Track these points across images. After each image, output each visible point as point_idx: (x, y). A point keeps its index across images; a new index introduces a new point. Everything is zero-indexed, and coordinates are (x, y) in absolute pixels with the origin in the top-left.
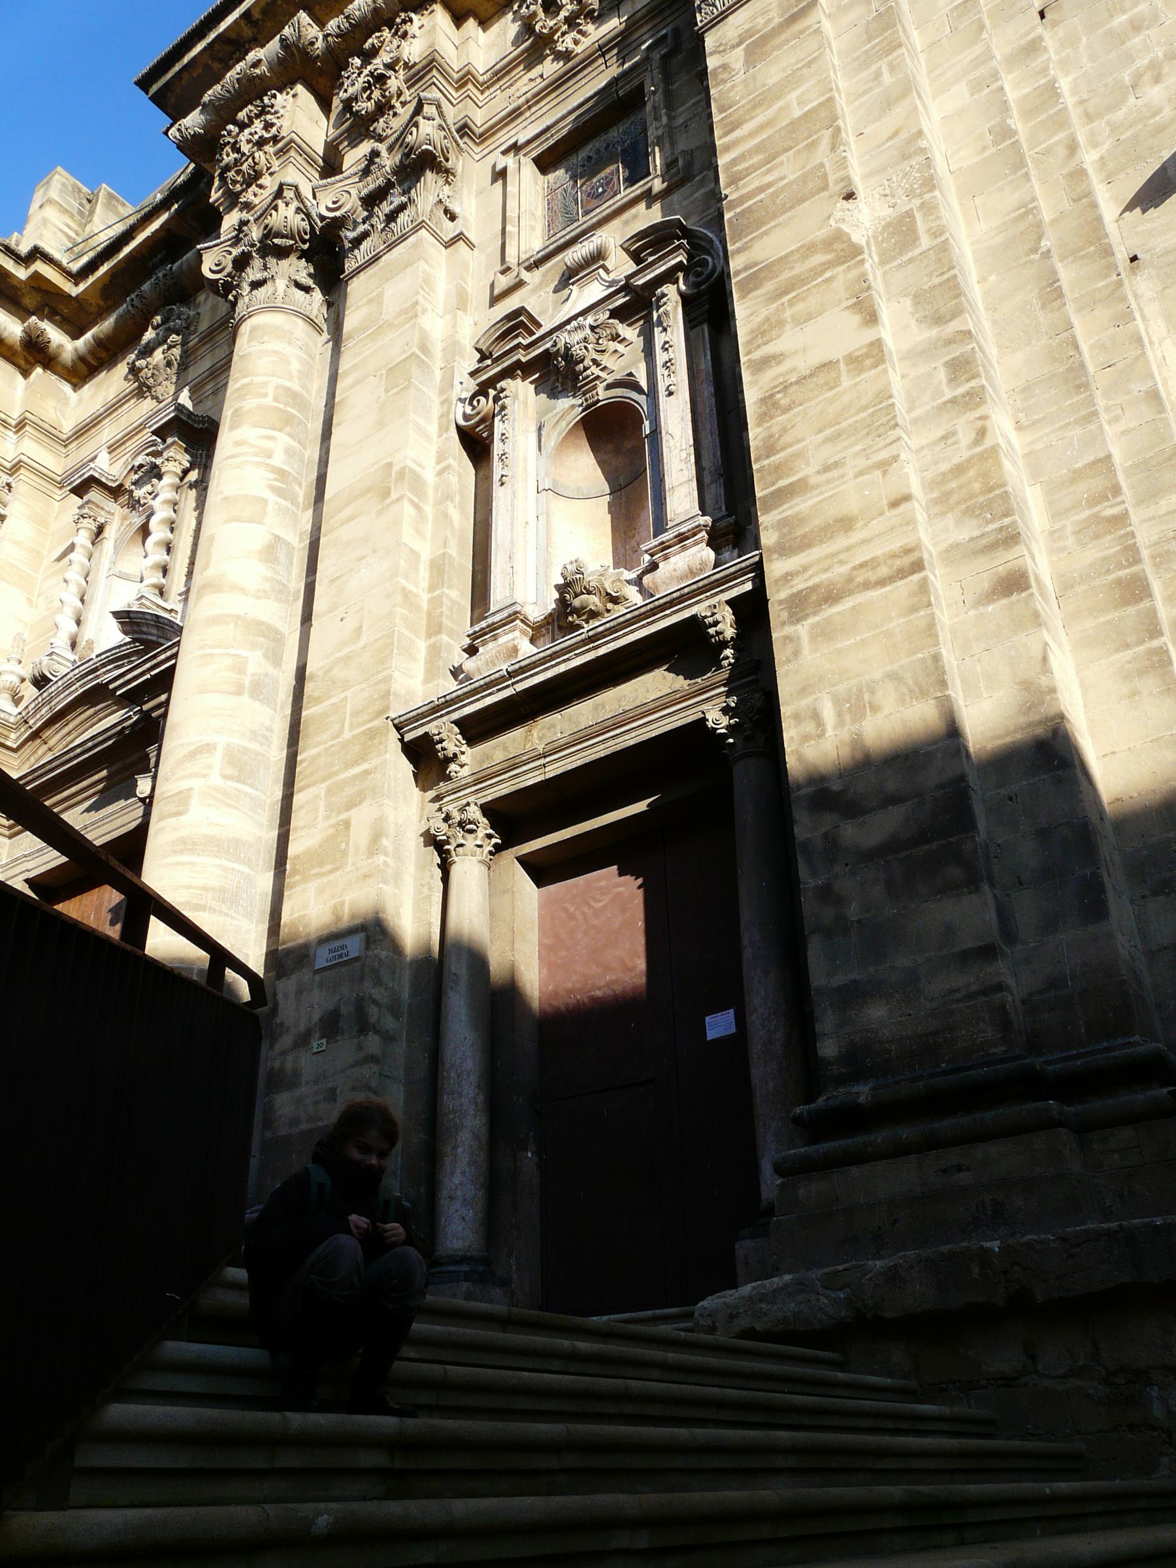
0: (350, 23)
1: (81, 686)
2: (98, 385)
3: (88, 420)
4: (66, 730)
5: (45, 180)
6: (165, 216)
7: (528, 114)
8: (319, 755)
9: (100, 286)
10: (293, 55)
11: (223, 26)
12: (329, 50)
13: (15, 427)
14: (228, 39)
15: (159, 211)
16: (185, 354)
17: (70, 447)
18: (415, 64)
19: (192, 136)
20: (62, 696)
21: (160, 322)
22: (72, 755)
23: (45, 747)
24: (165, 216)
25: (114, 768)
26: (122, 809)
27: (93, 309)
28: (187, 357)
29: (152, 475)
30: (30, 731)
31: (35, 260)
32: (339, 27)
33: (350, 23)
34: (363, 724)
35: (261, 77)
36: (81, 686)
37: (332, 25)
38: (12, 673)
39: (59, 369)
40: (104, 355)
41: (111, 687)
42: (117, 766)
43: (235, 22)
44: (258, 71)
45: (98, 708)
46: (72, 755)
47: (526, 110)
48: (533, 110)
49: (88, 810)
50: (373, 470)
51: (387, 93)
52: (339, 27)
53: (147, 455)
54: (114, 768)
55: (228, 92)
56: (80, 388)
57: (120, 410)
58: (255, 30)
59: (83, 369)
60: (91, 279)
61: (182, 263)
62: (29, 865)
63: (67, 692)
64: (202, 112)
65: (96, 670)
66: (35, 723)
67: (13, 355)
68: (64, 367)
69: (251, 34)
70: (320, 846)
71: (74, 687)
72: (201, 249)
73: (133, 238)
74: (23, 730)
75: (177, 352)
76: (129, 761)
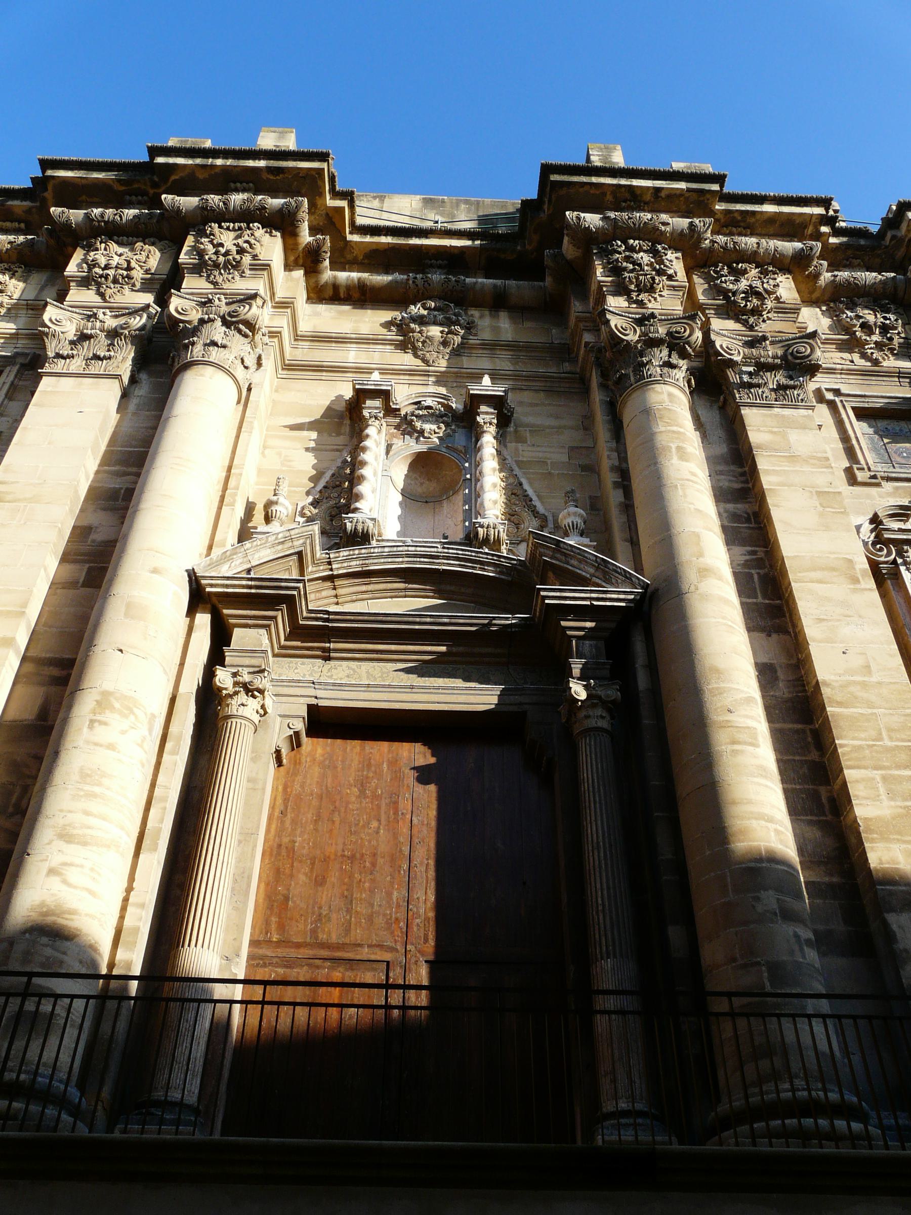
0: (735, 247)
1: (408, 562)
2: (341, 313)
3: (334, 335)
4: (364, 588)
5: (281, 129)
6: (468, 243)
7: (839, 376)
8: (860, 747)
9: (374, 247)
10: (692, 237)
11: (636, 182)
12: (711, 250)
13: (277, 303)
14: (634, 192)
15: (464, 235)
16: (462, 345)
17: (300, 343)
18: (784, 303)
19: (585, 227)
20: (382, 560)
21: (433, 307)
22: (418, 620)
23: (333, 592)
24: (468, 243)
25: (454, 649)
26: (467, 689)
27: (349, 257)
28: (462, 348)
29: (441, 420)
30: (331, 573)
31: (345, 199)
32: (726, 244)
33: (735, 247)
34: (903, 740)
35: (663, 233)
36: (408, 562)
37: (721, 239)
38: (287, 508)
39: (312, 281)
40: (356, 295)
41: (542, 593)
42: (461, 649)
43: (648, 188)
44: (663, 228)
45: (410, 586)
46: (418, 620)
47: (838, 373)
48: (843, 376)
49: (407, 671)
50: (832, 556)
51: (764, 306)
52: (726, 244)
53: (439, 403)
54: (454, 649)
55: (635, 225)
56: (313, 303)
57: (371, 346)
58: (653, 199)
59: (330, 292)
60: (368, 239)
61: (476, 283)
62: (320, 693)
63: (390, 560)
64: (602, 219)
65: (437, 557)
66: (338, 569)
67: (292, 250)
68: (317, 282)
69: (648, 200)
70: (893, 818)
71: (401, 560)
72: (607, 310)
73: (427, 238)
74: (322, 568)
75: (458, 340)
76: (477, 650)
